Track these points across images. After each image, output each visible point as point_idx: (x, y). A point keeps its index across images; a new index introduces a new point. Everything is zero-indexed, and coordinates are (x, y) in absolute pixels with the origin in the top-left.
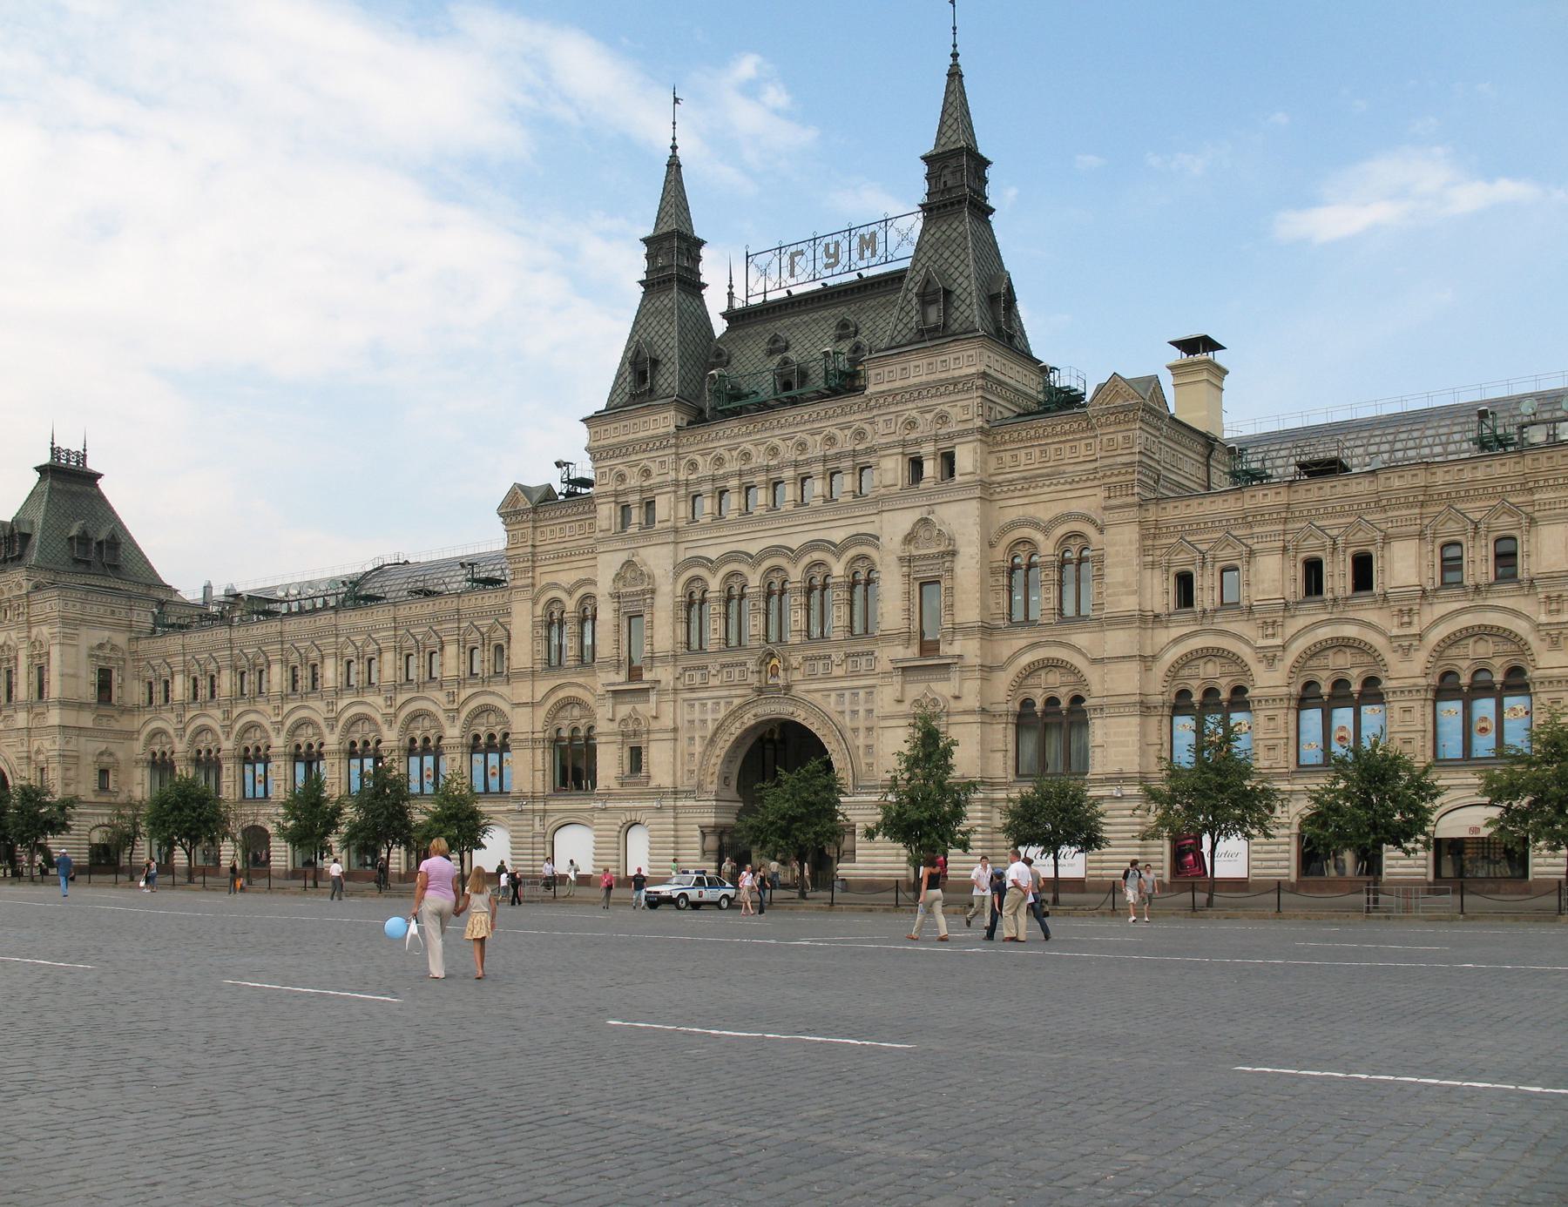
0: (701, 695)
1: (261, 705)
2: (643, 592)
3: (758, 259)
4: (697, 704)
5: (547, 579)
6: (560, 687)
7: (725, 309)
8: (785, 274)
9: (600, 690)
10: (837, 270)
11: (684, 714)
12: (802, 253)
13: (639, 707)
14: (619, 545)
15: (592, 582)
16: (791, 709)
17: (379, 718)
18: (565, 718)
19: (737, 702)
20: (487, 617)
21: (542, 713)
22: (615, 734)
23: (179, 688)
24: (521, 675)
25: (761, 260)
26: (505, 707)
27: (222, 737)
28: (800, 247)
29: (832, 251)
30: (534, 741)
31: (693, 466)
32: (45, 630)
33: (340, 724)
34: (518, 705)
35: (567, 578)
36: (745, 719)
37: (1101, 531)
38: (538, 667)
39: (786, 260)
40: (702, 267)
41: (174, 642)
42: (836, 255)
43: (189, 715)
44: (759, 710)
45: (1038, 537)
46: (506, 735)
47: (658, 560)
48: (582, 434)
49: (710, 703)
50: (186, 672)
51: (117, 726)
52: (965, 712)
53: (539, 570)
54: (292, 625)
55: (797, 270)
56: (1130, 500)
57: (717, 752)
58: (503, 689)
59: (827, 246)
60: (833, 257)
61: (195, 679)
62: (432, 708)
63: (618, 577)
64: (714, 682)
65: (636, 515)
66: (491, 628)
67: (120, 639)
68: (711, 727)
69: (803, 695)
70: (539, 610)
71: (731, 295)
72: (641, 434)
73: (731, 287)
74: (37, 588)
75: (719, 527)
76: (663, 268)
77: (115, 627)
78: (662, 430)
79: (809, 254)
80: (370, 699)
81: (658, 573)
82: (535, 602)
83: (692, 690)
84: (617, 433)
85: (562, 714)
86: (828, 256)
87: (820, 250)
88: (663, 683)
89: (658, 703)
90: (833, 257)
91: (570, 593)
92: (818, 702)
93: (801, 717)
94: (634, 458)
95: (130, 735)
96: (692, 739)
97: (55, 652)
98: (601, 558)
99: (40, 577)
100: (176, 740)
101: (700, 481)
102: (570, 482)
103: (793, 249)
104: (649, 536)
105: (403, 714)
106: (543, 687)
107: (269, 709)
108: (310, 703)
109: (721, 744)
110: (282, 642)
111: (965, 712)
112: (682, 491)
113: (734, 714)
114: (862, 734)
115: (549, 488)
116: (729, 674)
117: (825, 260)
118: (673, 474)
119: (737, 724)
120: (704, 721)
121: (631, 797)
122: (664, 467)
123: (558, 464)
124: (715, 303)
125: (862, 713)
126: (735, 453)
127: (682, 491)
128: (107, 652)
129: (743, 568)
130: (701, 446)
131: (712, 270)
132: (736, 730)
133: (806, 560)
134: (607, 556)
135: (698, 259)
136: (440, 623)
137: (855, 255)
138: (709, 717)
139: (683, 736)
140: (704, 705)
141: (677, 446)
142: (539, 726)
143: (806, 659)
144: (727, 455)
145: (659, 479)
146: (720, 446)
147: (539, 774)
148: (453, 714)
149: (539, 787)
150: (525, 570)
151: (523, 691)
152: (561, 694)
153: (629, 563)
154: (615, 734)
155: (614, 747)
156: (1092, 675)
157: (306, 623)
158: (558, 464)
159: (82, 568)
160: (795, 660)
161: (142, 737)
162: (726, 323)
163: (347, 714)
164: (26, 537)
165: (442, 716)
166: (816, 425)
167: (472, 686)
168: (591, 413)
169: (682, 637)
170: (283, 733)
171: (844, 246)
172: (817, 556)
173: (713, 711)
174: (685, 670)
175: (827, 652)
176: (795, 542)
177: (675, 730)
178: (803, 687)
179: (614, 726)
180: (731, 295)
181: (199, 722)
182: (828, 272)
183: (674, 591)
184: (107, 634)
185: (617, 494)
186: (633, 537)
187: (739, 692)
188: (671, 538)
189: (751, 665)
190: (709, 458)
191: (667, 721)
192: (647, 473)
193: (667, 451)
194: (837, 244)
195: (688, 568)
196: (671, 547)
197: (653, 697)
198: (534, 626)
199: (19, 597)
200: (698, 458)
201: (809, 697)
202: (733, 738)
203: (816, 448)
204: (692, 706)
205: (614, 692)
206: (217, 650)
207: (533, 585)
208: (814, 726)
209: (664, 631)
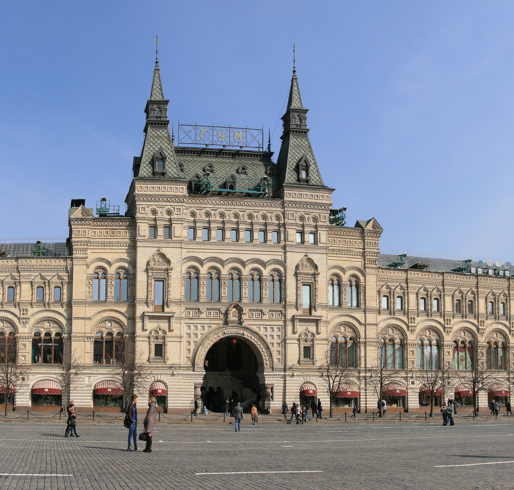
2: (167, 270)
37: (364, 275)
45: (341, 273)
52: (323, 340)
56: (375, 266)
83: (191, 319)
92: (262, 328)
93: (247, 335)
96: (189, 342)
109: (206, 345)
111: (323, 340)
114: (275, 345)
119: (215, 337)
120: (196, 335)
125: (275, 337)
129: (219, 266)
132: (214, 339)
138: (199, 332)
139: (184, 340)
143: (250, 310)
156: (361, 329)
160: (246, 310)
175: (261, 308)
178: (249, 323)
208: (254, 340)
209: (177, 289)
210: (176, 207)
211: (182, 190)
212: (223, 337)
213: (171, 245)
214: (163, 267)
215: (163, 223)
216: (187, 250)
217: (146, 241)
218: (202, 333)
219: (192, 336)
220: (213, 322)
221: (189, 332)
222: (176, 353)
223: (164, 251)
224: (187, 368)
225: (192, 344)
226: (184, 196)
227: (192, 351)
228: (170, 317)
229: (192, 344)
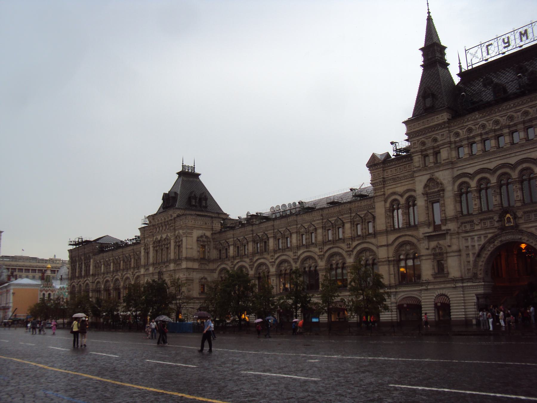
0: (471, 234)
2: (439, 191)
3: (470, 51)
4: (469, 239)
5: (390, 191)
6: (400, 237)
7: (458, 72)
8: (485, 54)
9: (421, 236)
10: (509, 48)
11: (463, 244)
12: (491, 44)
13: (441, 242)
14: (425, 173)
15: (415, 191)
16: (520, 237)
17: (316, 257)
18: (403, 250)
19: (490, 236)
20: (364, 210)
21: (392, 249)
22: (430, 255)
23: (232, 251)
24: (381, 233)
25: (472, 51)
26: (374, 248)
27: (249, 270)
28: (490, 42)
29: (506, 41)
30: (389, 261)
31: (457, 134)
33: (299, 261)
34: (381, 246)
35: (400, 189)
36: (496, 242)
38: (389, 229)
39: (484, 49)
40: (446, 57)
41: (230, 234)
42: (508, 42)
43: (236, 262)
44: (503, 238)
46: (374, 260)
47: (444, 176)
48: (404, 129)
49: (476, 238)
50: (235, 245)
51: (207, 268)
53: (386, 188)
54: (277, 222)
55: (490, 52)
57: (482, 259)
58: (373, 240)
59: (503, 40)
60: (507, 43)
62: (340, 251)
63: (426, 186)
64: (476, 228)
65: (431, 159)
66: (366, 215)
67: (208, 234)
68: (477, 248)
69: (525, 229)
70: (388, 205)
71: (460, 67)
72: (431, 124)
73: (460, 63)
75: (472, 159)
76: (431, 59)
77: (207, 229)
78: (441, 121)
79: (495, 44)
80: (312, 249)
81: (445, 182)
82: (385, 201)
83: (466, 232)
84: (419, 126)
85: (401, 249)
86: (505, 43)
87: (500, 42)
88: (452, 230)
89: (451, 239)
90: (507, 43)
91: (401, 196)
94: (429, 135)
95: (213, 271)
96: (468, 255)
97: (184, 239)
98: (417, 179)
99: (179, 212)
101: (461, 141)
102: (396, 150)
103: (487, 44)
104: (439, 167)
105: (327, 255)
106: (392, 238)
107: (269, 257)
109: (484, 255)
110: (274, 229)
112: (453, 146)
113: (490, 241)
115: (388, 155)
116: (485, 224)
117: (504, 45)
118: (448, 140)
119: (492, 246)
120: (473, 246)
121: (440, 283)
122: (442, 136)
123: (392, 143)
124: (454, 71)
126: (477, 126)
127: (453, 146)
128: (204, 239)
129: (487, 175)
130: (460, 126)
131: (451, 57)
133: (520, 168)
134: (420, 178)
135: (445, 54)
136: (342, 215)
137: (518, 41)
138: (476, 244)
139: (464, 253)
140: (473, 239)
141: (449, 127)
142: (391, 255)
143: (525, 213)
144: (473, 127)
145: (441, 142)
146: (470, 124)
147: (392, 276)
148: (349, 253)
149: (393, 281)
150: (380, 189)
151: (382, 240)
152: (401, 240)
153: (431, 180)
154: (430, 255)
155: (429, 261)
157: (283, 221)
158: (392, 143)
160: (519, 214)
161: (217, 272)
162: (459, 78)
163: (302, 257)
165: (344, 254)
166: (517, 108)
167: (358, 240)
168: (406, 119)
169: (459, 209)
170: (275, 266)
171: (512, 38)
172: (525, 165)
173: (478, 241)
174: (462, 223)
176: (513, 161)
177: (460, 251)
178: (525, 226)
179: (429, 252)
180: (460, 67)
181: (240, 264)
182: (506, 50)
183: (453, 189)
184: (204, 232)
185: (422, 151)
186: (430, 168)
187: (491, 231)
188: (450, 166)
189: (496, 218)
190: (465, 130)
191: (455, 248)
192: (435, 140)
193: (444, 130)
194: (508, 38)
195: (459, 179)
196: (450, 170)
197: (448, 237)
198: (386, 212)
199: (171, 220)
200: (459, 131)
201: (529, 230)
202: (489, 253)
203: (519, 117)
204: (467, 239)
205: (428, 236)
206: (247, 235)
207: (384, 194)
210: (440, 134)
211: (444, 117)
212: (499, 244)
213: (441, 169)
214: (436, 190)
215: (432, 151)
216: (457, 169)
217: (420, 170)
218: (479, 243)
219: (470, 247)
220: (488, 232)
221: (466, 245)
222: (454, 266)
223: (437, 175)
224: (469, 280)
225: (471, 255)
226: (444, 122)
227: (471, 262)
228: (445, 234)
229: (471, 255)
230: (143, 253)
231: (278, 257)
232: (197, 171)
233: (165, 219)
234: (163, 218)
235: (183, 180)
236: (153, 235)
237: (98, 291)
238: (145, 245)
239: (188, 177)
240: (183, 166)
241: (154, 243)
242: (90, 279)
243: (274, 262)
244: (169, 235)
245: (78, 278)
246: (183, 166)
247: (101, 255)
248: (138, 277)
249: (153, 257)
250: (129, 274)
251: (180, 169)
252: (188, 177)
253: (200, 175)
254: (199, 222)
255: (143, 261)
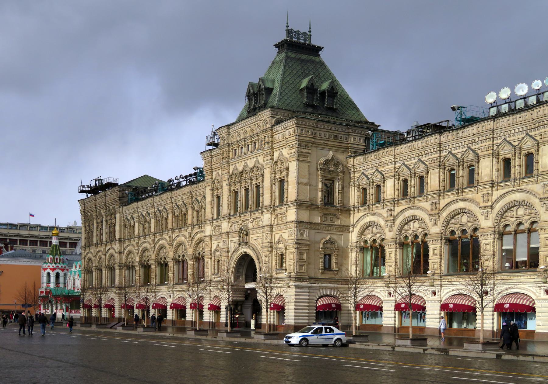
1: (470, 193)
27: (430, 224)
32: (285, 152)
41: (387, 155)
43: (398, 209)
50: (396, 175)
51: (338, 222)
61: (405, 181)
74: (278, 122)
100: (387, 230)
108: (523, 187)
159: (310, 110)
161: (357, 229)
164: (269, 91)
181: (407, 214)
230: (209, 198)
231: (502, 196)
232: (315, 42)
233: (252, 130)
234: (248, 130)
235: (287, 57)
236: (228, 162)
237: (130, 267)
238: (213, 183)
239: (299, 49)
240: (289, 32)
241: (231, 177)
242: (116, 246)
243: (492, 207)
244: (261, 159)
245: (97, 245)
246: (288, 31)
247: (134, 205)
248: (201, 241)
249: (229, 203)
250: (183, 237)
251: (283, 36)
252: (299, 49)
253: (320, 49)
254: (323, 134)
255: (209, 212)
